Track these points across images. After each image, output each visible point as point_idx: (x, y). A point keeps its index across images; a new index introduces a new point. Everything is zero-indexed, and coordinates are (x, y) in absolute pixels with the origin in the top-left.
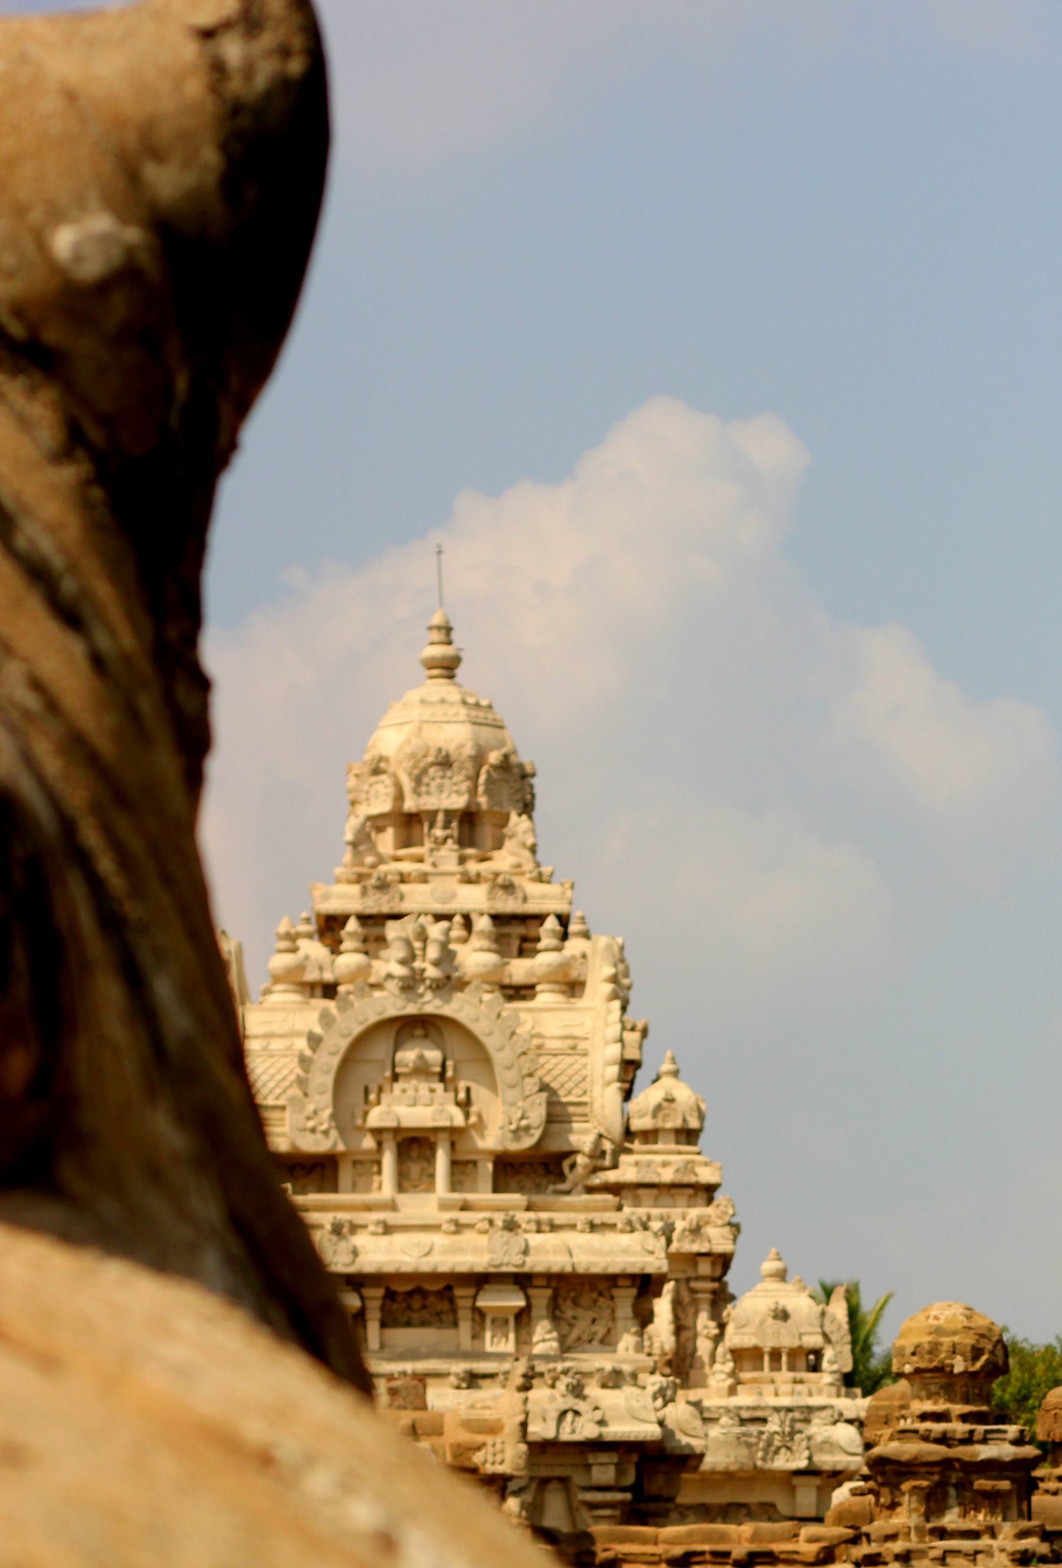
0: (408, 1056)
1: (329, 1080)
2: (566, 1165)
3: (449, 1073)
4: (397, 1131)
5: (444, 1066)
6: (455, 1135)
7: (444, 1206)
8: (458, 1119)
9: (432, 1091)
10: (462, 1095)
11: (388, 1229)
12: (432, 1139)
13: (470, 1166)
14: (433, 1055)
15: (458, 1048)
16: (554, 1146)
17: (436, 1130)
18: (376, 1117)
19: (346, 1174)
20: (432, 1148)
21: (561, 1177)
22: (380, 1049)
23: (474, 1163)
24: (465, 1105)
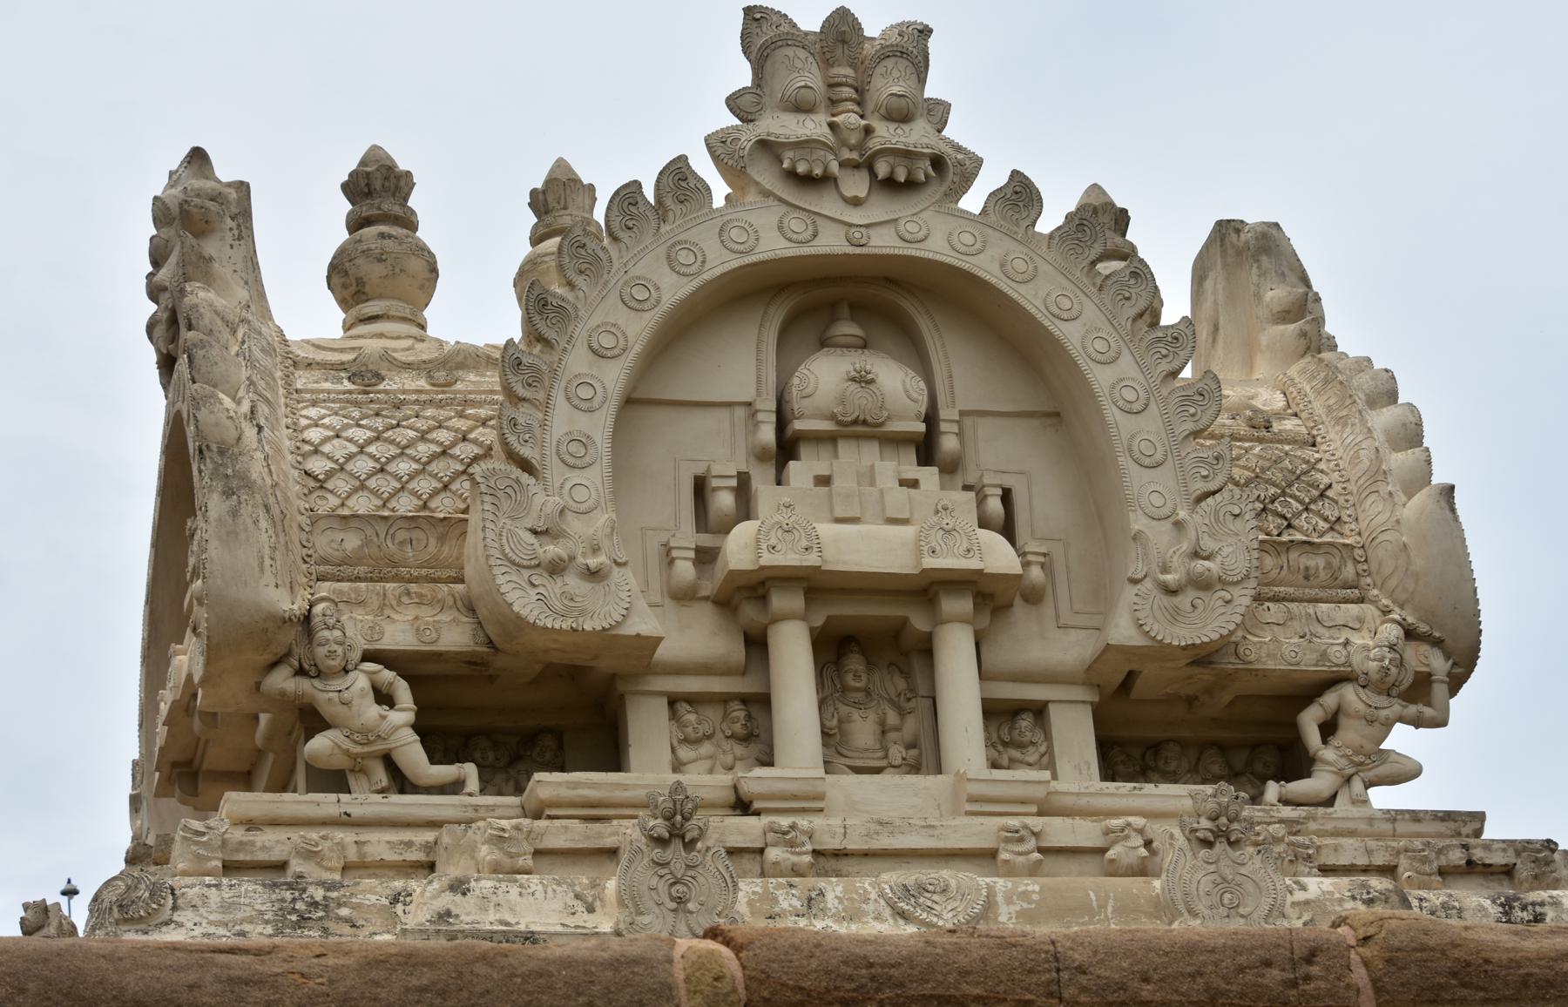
0: (825, 378)
1: (599, 427)
2: (1309, 721)
3: (948, 443)
4: (815, 585)
5: (931, 419)
6: (991, 598)
7: (981, 804)
8: (998, 556)
9: (913, 484)
10: (995, 505)
11: (830, 859)
12: (919, 622)
13: (1025, 722)
14: (896, 384)
15: (966, 376)
16: (1282, 647)
17: (929, 589)
18: (741, 548)
19: (649, 730)
20: (909, 656)
21: (1295, 763)
22: (738, 366)
23: (1039, 711)
24: (1008, 530)
